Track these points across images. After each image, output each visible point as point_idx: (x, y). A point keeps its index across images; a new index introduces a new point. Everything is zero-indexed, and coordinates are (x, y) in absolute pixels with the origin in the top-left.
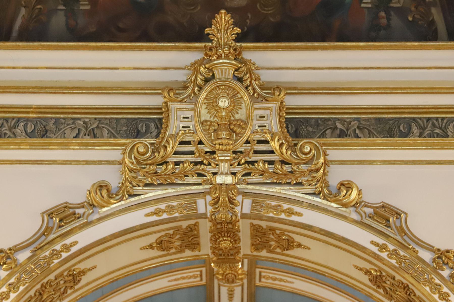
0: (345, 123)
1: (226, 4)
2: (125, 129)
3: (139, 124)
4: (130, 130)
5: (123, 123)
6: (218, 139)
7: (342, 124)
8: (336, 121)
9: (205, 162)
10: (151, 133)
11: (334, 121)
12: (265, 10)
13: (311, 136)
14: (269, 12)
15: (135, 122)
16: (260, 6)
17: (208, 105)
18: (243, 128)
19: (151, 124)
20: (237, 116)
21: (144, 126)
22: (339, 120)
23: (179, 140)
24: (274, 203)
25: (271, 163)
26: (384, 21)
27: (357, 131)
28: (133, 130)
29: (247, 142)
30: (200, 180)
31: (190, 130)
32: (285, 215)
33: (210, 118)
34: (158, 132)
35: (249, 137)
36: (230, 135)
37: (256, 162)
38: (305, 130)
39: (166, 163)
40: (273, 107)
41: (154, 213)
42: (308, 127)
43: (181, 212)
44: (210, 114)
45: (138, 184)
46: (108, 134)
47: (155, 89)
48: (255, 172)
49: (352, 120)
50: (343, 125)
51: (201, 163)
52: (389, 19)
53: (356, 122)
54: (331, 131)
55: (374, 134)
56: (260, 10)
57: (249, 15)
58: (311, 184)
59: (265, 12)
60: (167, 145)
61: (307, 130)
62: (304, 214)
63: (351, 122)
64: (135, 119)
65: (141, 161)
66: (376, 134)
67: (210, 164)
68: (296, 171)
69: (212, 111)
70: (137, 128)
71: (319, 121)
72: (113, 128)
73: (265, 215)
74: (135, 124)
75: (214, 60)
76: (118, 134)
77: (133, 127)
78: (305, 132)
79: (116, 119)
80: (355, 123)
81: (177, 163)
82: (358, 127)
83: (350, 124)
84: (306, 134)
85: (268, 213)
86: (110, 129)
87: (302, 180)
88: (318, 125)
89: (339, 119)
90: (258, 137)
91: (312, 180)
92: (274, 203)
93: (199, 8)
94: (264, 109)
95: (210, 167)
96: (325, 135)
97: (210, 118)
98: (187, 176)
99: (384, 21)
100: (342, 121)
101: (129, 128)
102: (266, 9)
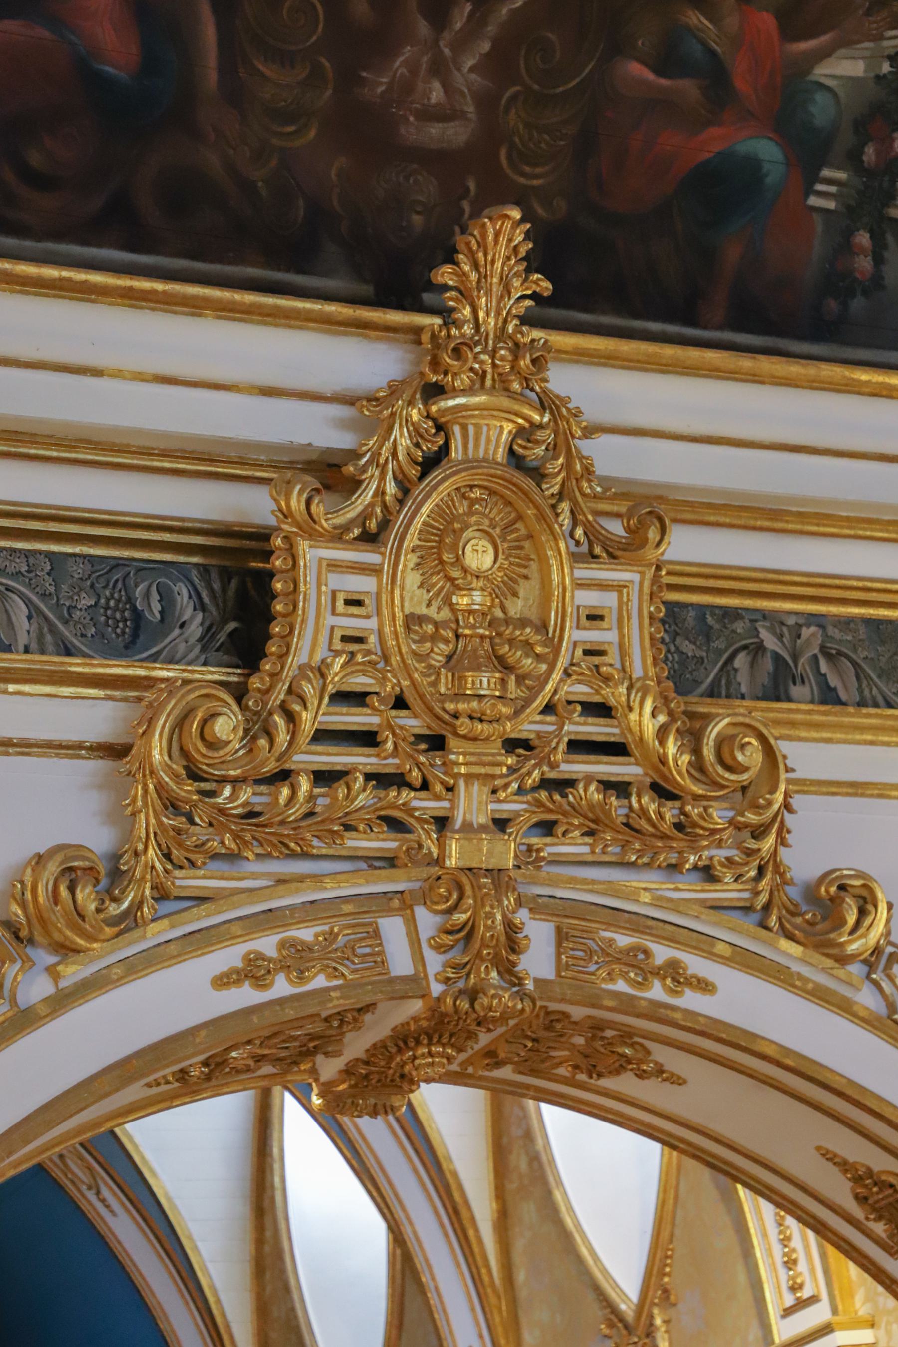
0: (785, 629)
1: (403, 131)
2: (87, 601)
3: (136, 586)
4: (107, 608)
5: (77, 576)
6: (460, 696)
7: (774, 633)
8: (756, 621)
9: (415, 776)
10: (182, 626)
11: (752, 621)
12: (523, 174)
13: (691, 673)
14: (535, 182)
15: (118, 575)
16: (509, 157)
17: (421, 557)
18: (539, 657)
19: (176, 589)
20: (516, 608)
21: (155, 596)
22: (765, 617)
23: (331, 689)
24: (623, 941)
25: (621, 788)
26: (864, 264)
27: (824, 667)
28: (116, 609)
29: (549, 709)
30: (386, 843)
31: (369, 652)
32: (664, 986)
33: (429, 605)
34: (207, 623)
35: (555, 692)
36: (503, 682)
37: (570, 783)
38: (673, 648)
39: (284, 776)
40: (632, 582)
41: (246, 976)
42: (679, 640)
43: (335, 973)
44: (428, 591)
45: (192, 856)
46: (30, 618)
47: (211, 461)
48: (568, 823)
49: (801, 621)
50: (780, 637)
51: (398, 780)
52: (878, 260)
53: (813, 629)
54: (749, 658)
55: (872, 680)
56: (508, 171)
57: (472, 185)
58: (741, 875)
59: (522, 180)
60: (297, 708)
61: (677, 648)
62: (717, 983)
63: (799, 626)
64: (118, 563)
65: (204, 767)
66: (873, 676)
67: (425, 786)
68: (695, 825)
69: (434, 579)
70: (130, 600)
71: (710, 620)
72: (44, 596)
73: (604, 986)
74: (120, 585)
75: (456, 392)
76: (66, 622)
77: (116, 595)
78: (674, 659)
79: (50, 555)
80: (813, 635)
81: (323, 777)
82: (823, 649)
83: (799, 636)
84: (676, 666)
85: (611, 980)
86: (34, 598)
87: (711, 858)
88: (708, 634)
89: (765, 615)
90: (581, 691)
91: (747, 864)
92: (623, 941)
93: (312, 133)
94: (602, 586)
95: (423, 794)
96: (732, 672)
97: (429, 605)
98: (355, 829)
99: (864, 264)
100: (774, 619)
101: (103, 601)
102: (527, 169)
